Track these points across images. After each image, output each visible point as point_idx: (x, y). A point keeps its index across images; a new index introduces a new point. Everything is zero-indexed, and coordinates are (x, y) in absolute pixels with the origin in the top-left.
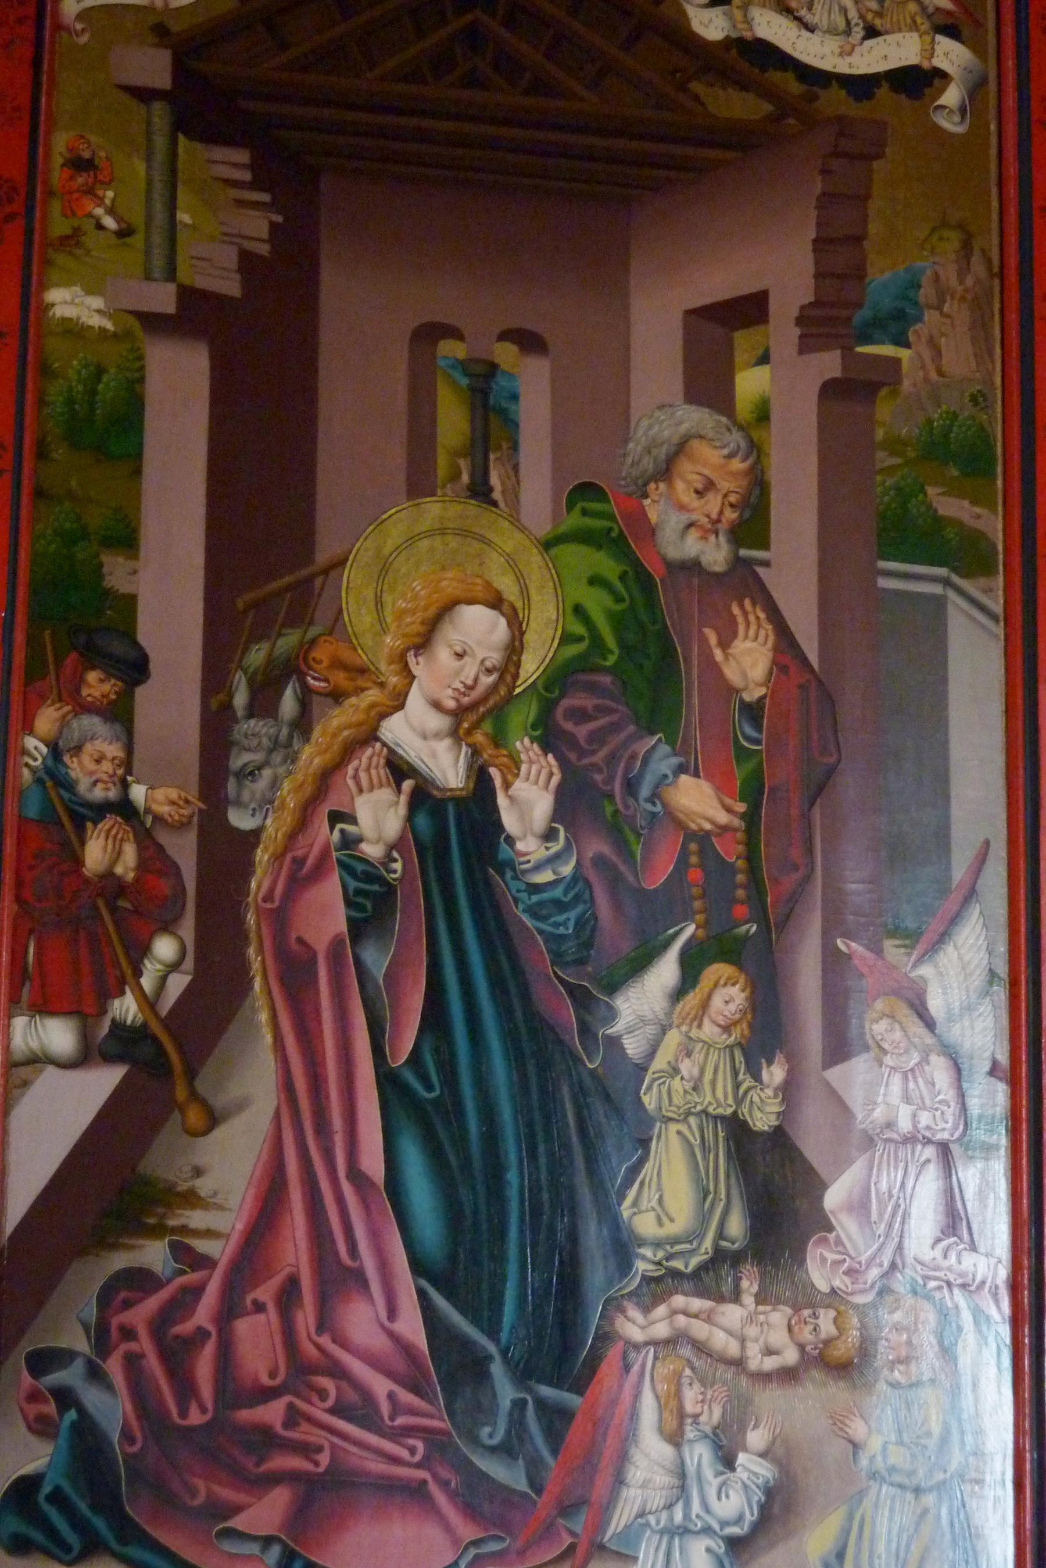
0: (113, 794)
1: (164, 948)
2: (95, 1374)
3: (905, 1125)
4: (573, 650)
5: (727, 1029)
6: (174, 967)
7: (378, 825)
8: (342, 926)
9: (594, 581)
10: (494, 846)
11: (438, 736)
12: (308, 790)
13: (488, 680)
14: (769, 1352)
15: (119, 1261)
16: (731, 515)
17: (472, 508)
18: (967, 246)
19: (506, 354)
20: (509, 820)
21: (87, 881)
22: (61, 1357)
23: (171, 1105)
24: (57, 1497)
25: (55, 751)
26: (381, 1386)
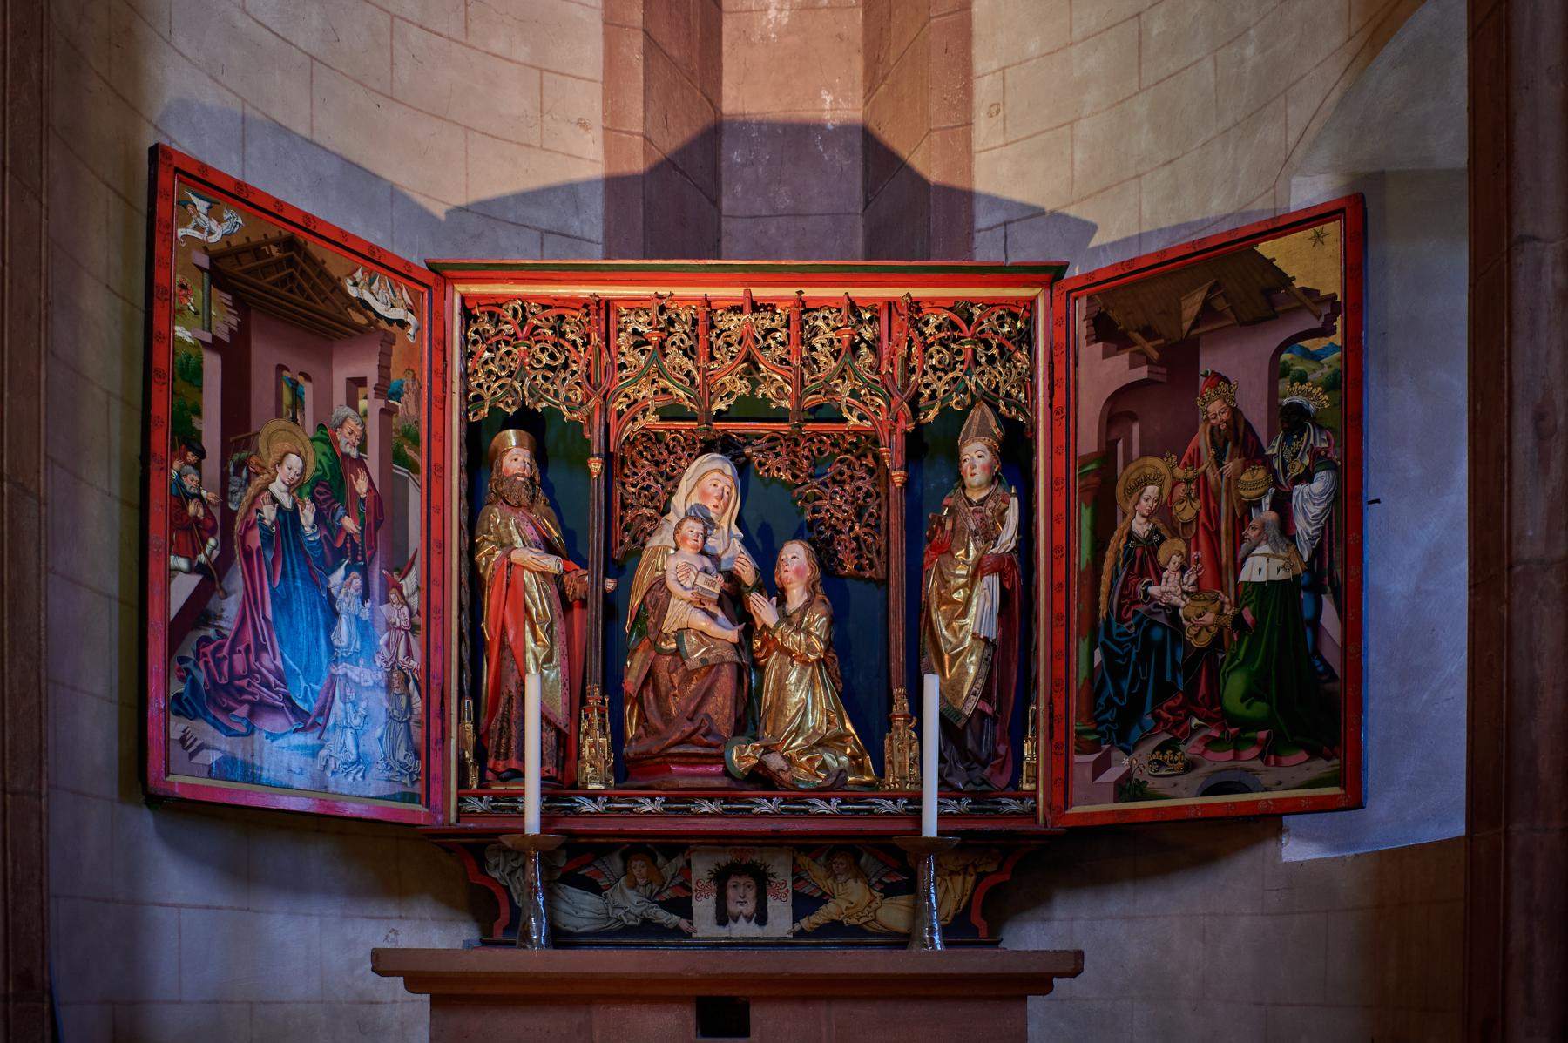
0: (196, 492)
1: (212, 542)
2: (196, 665)
3: (398, 624)
4: (319, 473)
5: (356, 590)
6: (215, 548)
7: (269, 515)
8: (260, 544)
9: (324, 454)
10: (299, 529)
11: (284, 492)
12: (250, 502)
13: (297, 478)
14: (366, 681)
15: (202, 633)
16: (357, 442)
17: (292, 425)
18: (414, 376)
19: (300, 379)
20: (303, 520)
21: (189, 517)
22: (186, 660)
23: (214, 589)
24: (186, 699)
25: (180, 475)
26: (272, 678)
